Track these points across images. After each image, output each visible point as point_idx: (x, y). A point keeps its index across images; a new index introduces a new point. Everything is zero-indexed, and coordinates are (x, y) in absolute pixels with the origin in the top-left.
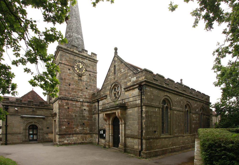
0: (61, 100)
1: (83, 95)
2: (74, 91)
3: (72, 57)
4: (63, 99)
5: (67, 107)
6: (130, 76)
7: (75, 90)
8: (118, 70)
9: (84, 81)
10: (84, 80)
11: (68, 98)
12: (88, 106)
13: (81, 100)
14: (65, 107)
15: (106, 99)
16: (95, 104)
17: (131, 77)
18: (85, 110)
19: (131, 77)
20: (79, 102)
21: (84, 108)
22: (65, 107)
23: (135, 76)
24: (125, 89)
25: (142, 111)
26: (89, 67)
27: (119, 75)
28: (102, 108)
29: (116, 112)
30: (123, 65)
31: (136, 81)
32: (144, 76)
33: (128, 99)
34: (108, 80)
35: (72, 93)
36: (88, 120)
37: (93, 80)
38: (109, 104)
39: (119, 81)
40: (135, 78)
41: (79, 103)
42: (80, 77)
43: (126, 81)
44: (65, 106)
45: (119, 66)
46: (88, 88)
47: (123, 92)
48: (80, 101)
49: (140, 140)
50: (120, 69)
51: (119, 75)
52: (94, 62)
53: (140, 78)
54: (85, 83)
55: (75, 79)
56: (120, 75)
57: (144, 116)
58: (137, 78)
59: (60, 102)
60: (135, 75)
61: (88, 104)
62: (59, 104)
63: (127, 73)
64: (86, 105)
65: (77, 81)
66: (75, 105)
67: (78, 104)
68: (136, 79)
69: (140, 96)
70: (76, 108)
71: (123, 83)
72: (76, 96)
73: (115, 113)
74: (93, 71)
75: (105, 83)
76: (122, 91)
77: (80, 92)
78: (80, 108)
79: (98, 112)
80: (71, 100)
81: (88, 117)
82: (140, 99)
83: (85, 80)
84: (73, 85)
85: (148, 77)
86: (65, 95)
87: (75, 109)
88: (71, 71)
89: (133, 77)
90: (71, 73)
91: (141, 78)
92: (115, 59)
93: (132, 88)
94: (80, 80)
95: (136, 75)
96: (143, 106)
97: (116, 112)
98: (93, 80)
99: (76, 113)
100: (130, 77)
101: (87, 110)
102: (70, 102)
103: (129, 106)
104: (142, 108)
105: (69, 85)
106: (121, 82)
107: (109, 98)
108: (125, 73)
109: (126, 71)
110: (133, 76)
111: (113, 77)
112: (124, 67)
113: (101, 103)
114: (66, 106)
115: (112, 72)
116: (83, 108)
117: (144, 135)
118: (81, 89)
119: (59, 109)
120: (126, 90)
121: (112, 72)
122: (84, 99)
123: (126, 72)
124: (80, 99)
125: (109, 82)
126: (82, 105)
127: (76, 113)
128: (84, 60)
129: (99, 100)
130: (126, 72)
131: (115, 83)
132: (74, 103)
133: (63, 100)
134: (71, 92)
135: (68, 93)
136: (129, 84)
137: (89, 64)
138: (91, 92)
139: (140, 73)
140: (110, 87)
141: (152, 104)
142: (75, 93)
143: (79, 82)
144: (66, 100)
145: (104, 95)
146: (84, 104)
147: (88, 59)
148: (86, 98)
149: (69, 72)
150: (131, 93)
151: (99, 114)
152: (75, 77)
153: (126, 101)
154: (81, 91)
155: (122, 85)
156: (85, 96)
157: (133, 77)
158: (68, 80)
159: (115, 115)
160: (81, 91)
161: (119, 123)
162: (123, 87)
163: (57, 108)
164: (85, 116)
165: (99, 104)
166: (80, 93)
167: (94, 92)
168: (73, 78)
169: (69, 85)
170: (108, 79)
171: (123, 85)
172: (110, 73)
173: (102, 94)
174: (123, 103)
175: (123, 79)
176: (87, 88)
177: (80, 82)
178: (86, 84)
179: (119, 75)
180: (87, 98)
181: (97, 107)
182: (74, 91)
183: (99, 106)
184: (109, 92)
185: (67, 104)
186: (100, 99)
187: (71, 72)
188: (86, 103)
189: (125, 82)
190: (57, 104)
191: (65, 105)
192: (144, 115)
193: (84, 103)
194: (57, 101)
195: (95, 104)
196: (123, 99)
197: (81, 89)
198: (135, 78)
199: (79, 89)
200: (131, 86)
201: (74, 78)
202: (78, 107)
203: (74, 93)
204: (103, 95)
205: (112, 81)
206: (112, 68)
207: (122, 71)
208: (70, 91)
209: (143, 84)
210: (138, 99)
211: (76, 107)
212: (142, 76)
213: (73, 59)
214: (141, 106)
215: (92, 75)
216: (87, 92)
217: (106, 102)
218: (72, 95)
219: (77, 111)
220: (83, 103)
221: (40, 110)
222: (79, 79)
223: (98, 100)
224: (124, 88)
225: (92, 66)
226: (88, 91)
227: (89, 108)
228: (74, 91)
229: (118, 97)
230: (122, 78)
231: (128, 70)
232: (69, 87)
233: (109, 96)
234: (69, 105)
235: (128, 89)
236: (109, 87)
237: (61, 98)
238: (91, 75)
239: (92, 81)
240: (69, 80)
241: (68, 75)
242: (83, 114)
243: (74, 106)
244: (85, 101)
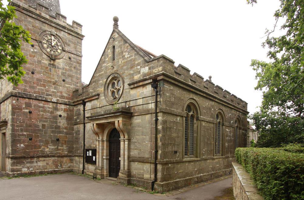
0: (16, 98)
1: (58, 92)
2: (42, 83)
3: (37, 25)
4: (20, 97)
5: (28, 111)
6: (138, 64)
7: (44, 82)
8: (119, 54)
9: (58, 68)
10: (59, 67)
11: (31, 94)
12: (65, 110)
13: (54, 100)
14: (23, 110)
15: (99, 100)
16: (79, 108)
17: (141, 67)
18: (60, 116)
19: (141, 67)
20: (51, 104)
21: (59, 113)
22: (23, 110)
23: (147, 66)
24: (129, 85)
25: (157, 120)
26: (69, 45)
27: (120, 62)
28: (92, 114)
29: (115, 121)
30: (128, 47)
31: (148, 74)
32: (161, 66)
33: (134, 101)
34: (102, 69)
35: (38, 87)
36: (67, 133)
37: (75, 68)
38: (102, 108)
39: (120, 72)
40: (147, 68)
41: (51, 105)
42: (52, 61)
43: (132, 72)
44: (24, 109)
45: (121, 48)
46: (67, 80)
47: (126, 89)
48: (53, 101)
49: (153, 166)
50: (122, 52)
51: (121, 62)
52: (79, 38)
53: (155, 69)
54: (61, 71)
55: (43, 63)
56: (123, 62)
57: (161, 128)
58: (149, 69)
59: (14, 102)
60: (147, 64)
61: (65, 108)
62: (13, 106)
63: (134, 60)
64: (62, 109)
65: (47, 68)
66: (43, 107)
67: (48, 106)
68: (148, 69)
69: (155, 96)
70: (44, 114)
71: (126, 76)
72: (44, 93)
73: (113, 123)
74: (75, 53)
75: (97, 74)
76: (124, 89)
77: (51, 86)
78: (52, 113)
79: (83, 120)
80: (35, 98)
81: (66, 128)
82: (154, 102)
83: (61, 66)
84: (39, 73)
85: (167, 68)
86: (25, 90)
87: (43, 114)
88: (36, 48)
89: (144, 67)
90: (36, 52)
91: (157, 69)
92: (115, 35)
93: (141, 84)
94: (52, 66)
95: (149, 63)
96: (158, 112)
97: (115, 121)
98: (75, 68)
99: (45, 121)
100: (139, 67)
101: (64, 117)
102: (33, 102)
103: (136, 112)
104: (156, 116)
105: (33, 73)
106: (123, 73)
107: (102, 97)
108: (130, 60)
109: (132, 56)
110: (143, 65)
111: (110, 64)
112: (129, 50)
113: (89, 105)
114: (27, 109)
115: (110, 56)
116: (57, 114)
117: (159, 157)
118: (53, 80)
119: (13, 113)
120: (132, 86)
121: (110, 56)
122: (58, 98)
123: (133, 57)
124: (52, 99)
125: (103, 72)
126: (56, 109)
127: (45, 122)
128: (60, 33)
129: (86, 101)
130: (133, 57)
131: (114, 74)
132: (41, 105)
133: (20, 99)
134: (35, 85)
135: (30, 87)
136: (137, 77)
137: (69, 41)
138: (72, 86)
139: (154, 61)
140: (106, 80)
141: (172, 110)
142: (43, 88)
143: (50, 69)
144: (26, 98)
145: (94, 94)
146: (58, 107)
147: (66, 31)
148: (62, 97)
149: (32, 50)
150: (140, 92)
151: (84, 124)
152: (43, 60)
153: (132, 104)
155: (126, 78)
156: (61, 93)
157: (144, 67)
158: (30, 64)
159: (113, 127)
160: (54, 84)
161: (120, 139)
162: (127, 82)
163: (9, 112)
164: (60, 126)
165: (86, 108)
166: (51, 88)
167: (77, 88)
168: (39, 62)
169: (33, 73)
170: (102, 67)
171: (127, 79)
172: (105, 58)
173: (91, 91)
174: (127, 106)
175: (127, 69)
176: (64, 81)
177: (53, 69)
178: (63, 74)
179: (120, 62)
180: (64, 96)
181: (82, 112)
182: (41, 84)
183: (85, 111)
184: (103, 89)
185: (28, 105)
186: (87, 100)
187: (35, 50)
188: (63, 105)
189: (130, 74)
190: (8, 104)
191: (24, 106)
192: (160, 127)
193: (59, 104)
194: (9, 100)
195: (79, 108)
196: (126, 101)
198: (147, 68)
200: (140, 81)
201: (42, 61)
202: (49, 111)
203: (41, 88)
204: (92, 93)
205: (108, 72)
206: (109, 51)
207: (126, 57)
209: (159, 78)
210: (150, 102)
211: (45, 111)
212: (157, 67)
213: (40, 29)
214: (156, 113)
215: (74, 58)
216: (64, 86)
217: (98, 104)
218: (37, 90)
219: (46, 118)
220: (57, 106)
222: (50, 64)
223: (83, 100)
224: (128, 83)
225: (75, 44)
226: (67, 85)
227: (67, 114)
228: (42, 83)
229: (118, 97)
230: (125, 67)
231: (135, 54)
232: (32, 76)
233: (103, 95)
234: (31, 107)
235: (136, 85)
236: (103, 81)
237: (18, 95)
238: (72, 59)
239: (73, 69)
240: (33, 64)
241: (30, 56)
242: (56, 123)
244: (60, 102)
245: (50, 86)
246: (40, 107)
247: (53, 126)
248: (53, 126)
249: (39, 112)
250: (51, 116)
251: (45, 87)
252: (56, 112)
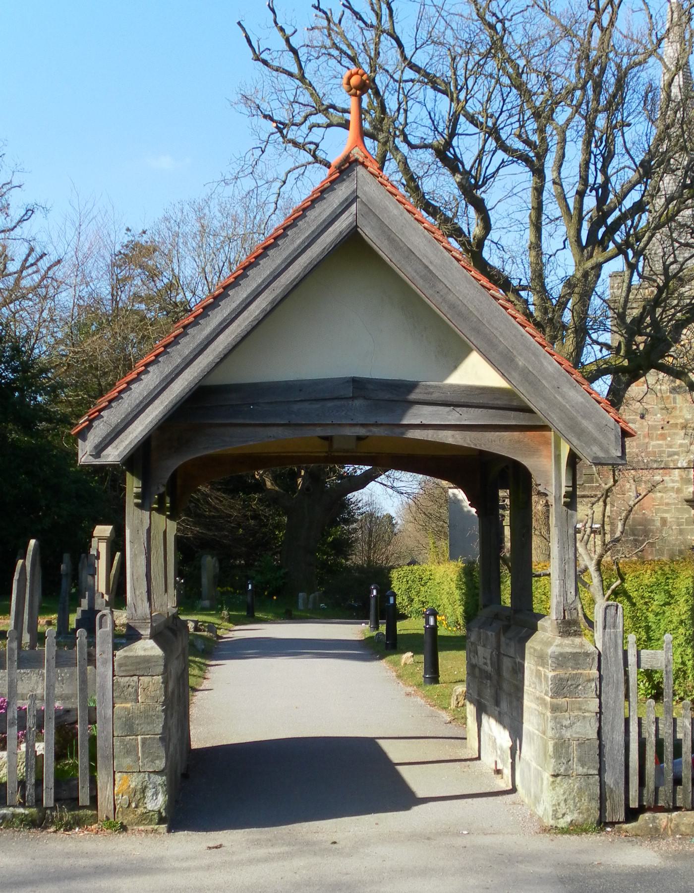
2: (659, 432)
35: (653, 443)
48: (679, 465)
72: (663, 452)
87: (662, 497)
118: (681, 421)
124: (678, 460)
134: (647, 440)
142: (661, 442)
143: (674, 399)
154: (682, 428)
166: (678, 437)
169: (642, 417)
197: (683, 421)
199: (677, 424)
202: (673, 488)
208: (644, 437)
219: (667, 504)
245: (675, 434)
247: (682, 518)
248: (682, 518)
250: (678, 497)
251: (665, 439)
252: (687, 488)
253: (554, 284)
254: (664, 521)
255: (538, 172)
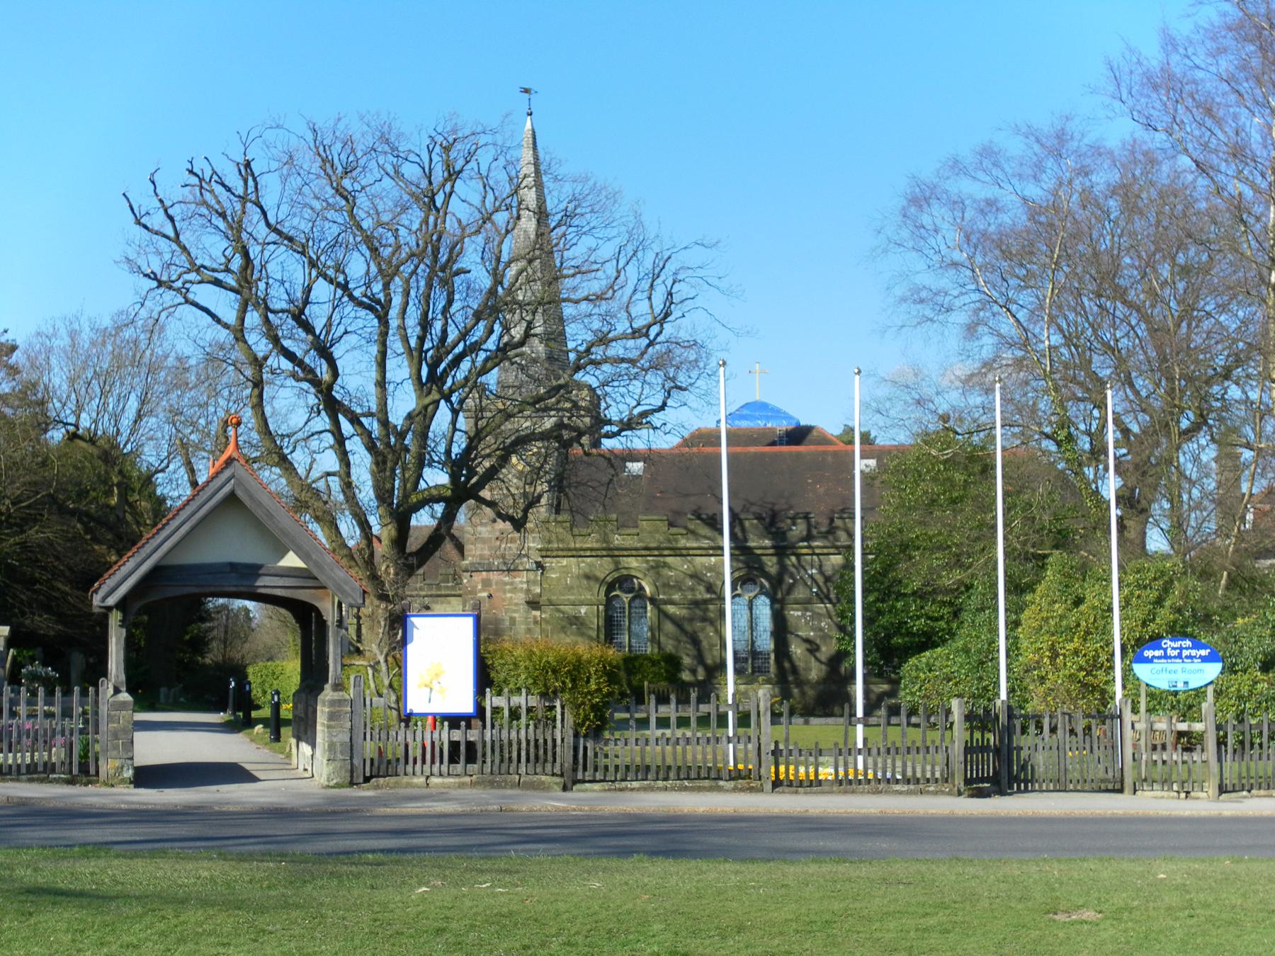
5: (485, 594)
14: (479, 595)
22: (479, 595)
44: (480, 591)
66: (512, 584)
185: (486, 583)
191: (480, 587)
219: (516, 604)
221: (442, 603)
234: (490, 585)
243: (508, 587)
246: (506, 584)
249: (505, 593)
253: (397, 417)
254: (513, 620)
255: (384, 321)
